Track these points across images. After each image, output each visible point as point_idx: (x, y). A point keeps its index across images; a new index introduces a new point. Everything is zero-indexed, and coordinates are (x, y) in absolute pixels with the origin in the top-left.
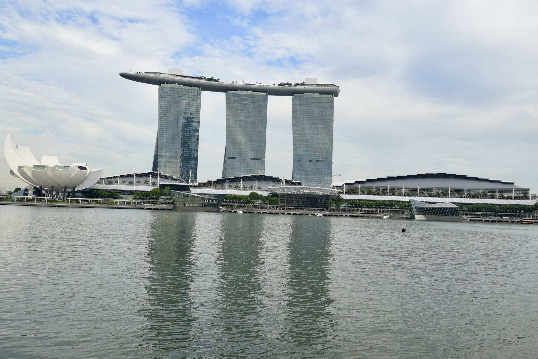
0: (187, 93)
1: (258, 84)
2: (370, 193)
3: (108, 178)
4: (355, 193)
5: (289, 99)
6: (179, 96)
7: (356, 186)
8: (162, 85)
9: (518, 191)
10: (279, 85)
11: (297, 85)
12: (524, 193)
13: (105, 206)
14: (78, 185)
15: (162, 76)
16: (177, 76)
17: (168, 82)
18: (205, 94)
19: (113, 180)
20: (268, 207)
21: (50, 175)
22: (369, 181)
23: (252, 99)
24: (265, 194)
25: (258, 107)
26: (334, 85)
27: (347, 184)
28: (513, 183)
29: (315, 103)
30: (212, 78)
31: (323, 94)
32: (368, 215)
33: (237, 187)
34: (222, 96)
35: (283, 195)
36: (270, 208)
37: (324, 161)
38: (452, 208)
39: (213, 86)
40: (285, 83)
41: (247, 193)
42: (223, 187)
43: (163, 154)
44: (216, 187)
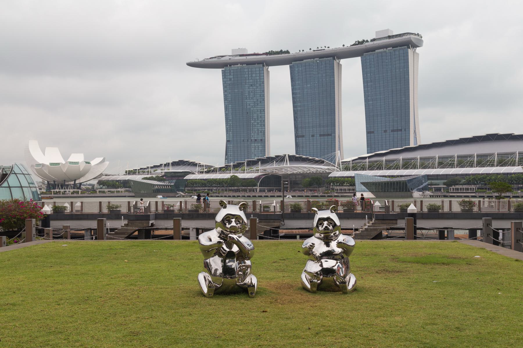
0: (250, 73)
1: (326, 49)
3: (141, 169)
5: (358, 59)
6: (242, 77)
11: (372, 41)
13: (86, 195)
14: (79, 178)
17: (231, 64)
18: (273, 70)
19: (146, 170)
20: (258, 190)
21: (46, 172)
23: (316, 67)
24: (253, 175)
25: (324, 75)
29: (389, 60)
30: (281, 51)
31: (397, 47)
32: (343, 194)
34: (286, 69)
35: (287, 176)
36: (260, 191)
37: (401, 130)
39: (277, 58)
40: (361, 40)
43: (231, 139)
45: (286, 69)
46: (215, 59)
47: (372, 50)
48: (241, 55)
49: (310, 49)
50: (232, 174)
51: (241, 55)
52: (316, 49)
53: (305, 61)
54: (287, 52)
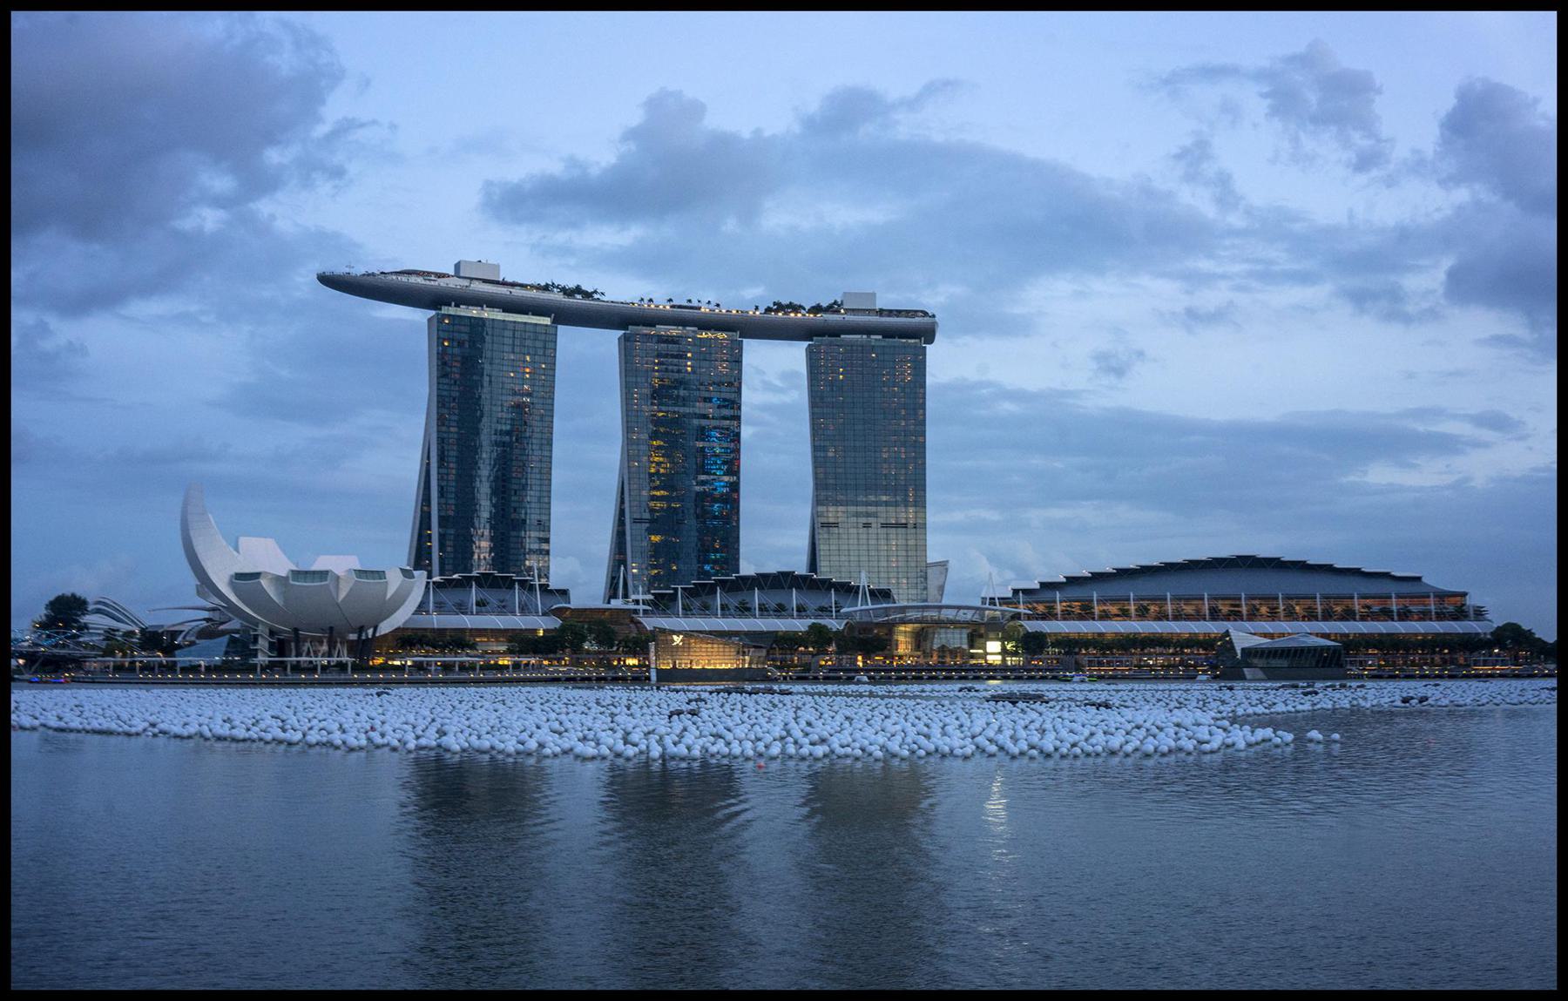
2: (1086, 613)
4: (1049, 615)
7: (1047, 595)
8: (445, 310)
9: (1442, 596)
10: (768, 310)
12: (1454, 606)
15: (442, 282)
16: (485, 281)
22: (1072, 581)
26: (925, 314)
27: (1026, 592)
28: (1419, 579)
33: (744, 610)
38: (1323, 649)
41: (800, 625)
42: (706, 610)
44: (688, 611)
46: (413, 279)
47: (834, 332)
50: (810, 621)
51: (485, 281)
53: (662, 330)
54: (588, 295)
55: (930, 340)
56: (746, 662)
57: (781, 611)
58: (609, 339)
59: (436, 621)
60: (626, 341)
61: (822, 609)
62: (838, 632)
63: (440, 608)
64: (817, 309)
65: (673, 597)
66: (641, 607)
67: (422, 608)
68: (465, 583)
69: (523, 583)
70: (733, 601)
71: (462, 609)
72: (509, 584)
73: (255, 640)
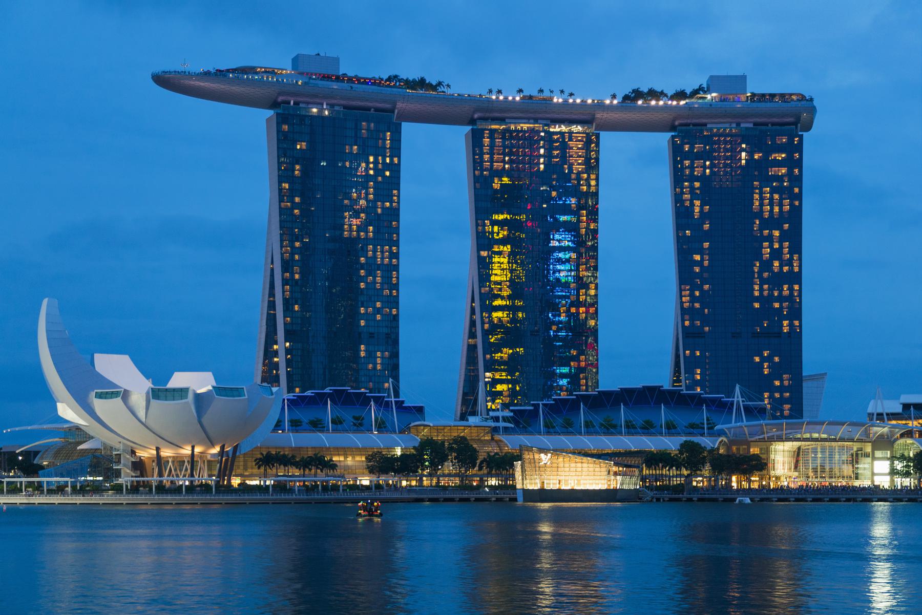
26: (802, 98)
41: (671, 444)
45: (456, 137)
48: (327, 77)
49: (520, 91)
51: (327, 77)
52: (535, 93)
54: (434, 88)
55: (808, 128)
56: (616, 483)
57: (648, 428)
58: (456, 137)
59: (292, 440)
60: (476, 139)
61: (692, 426)
62: (712, 451)
63: (296, 425)
64: (680, 95)
65: (534, 414)
66: (502, 424)
67: (279, 425)
68: (319, 400)
69: (379, 401)
70: (598, 419)
71: (317, 425)
72: (364, 401)
73: (119, 462)
